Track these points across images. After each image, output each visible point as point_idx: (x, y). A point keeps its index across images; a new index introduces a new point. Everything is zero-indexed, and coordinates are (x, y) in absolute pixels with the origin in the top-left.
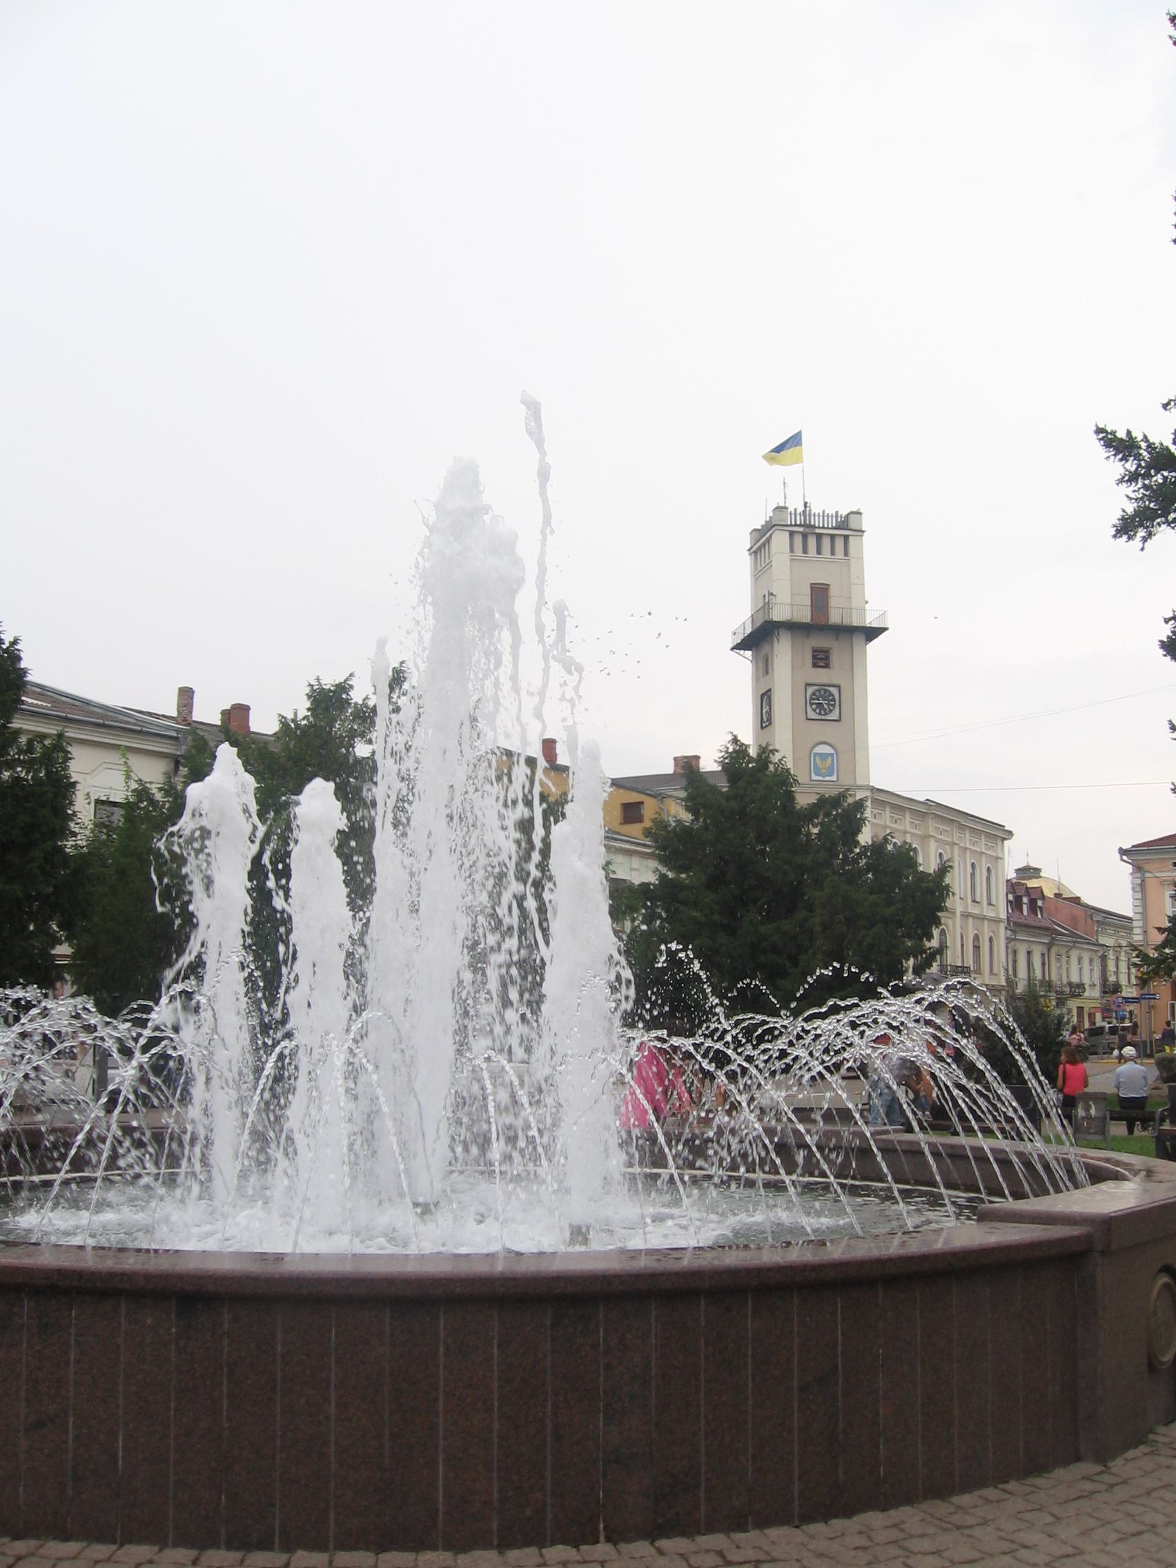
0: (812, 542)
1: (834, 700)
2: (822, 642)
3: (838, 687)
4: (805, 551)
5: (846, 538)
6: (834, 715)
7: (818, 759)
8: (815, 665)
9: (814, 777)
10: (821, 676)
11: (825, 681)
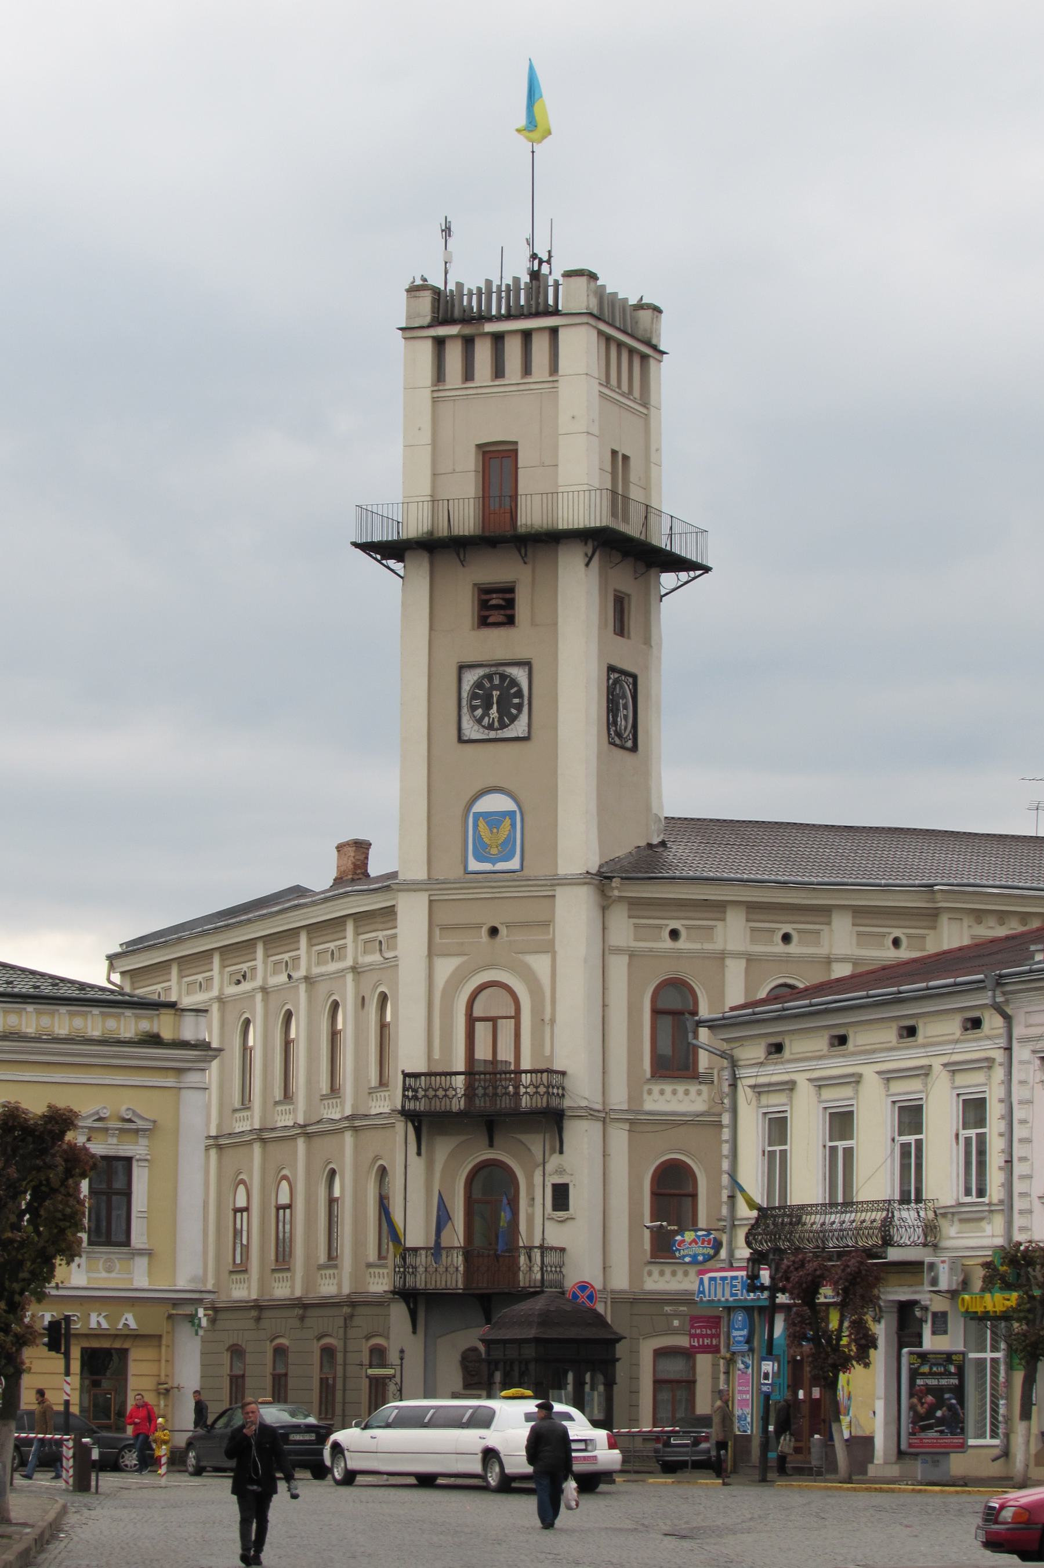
0: (483, 352)
1: (519, 694)
2: (494, 570)
3: (527, 664)
4: (468, 374)
5: (554, 331)
6: (520, 728)
7: (482, 824)
8: (483, 622)
9: (474, 865)
10: (495, 644)
11: (501, 655)
